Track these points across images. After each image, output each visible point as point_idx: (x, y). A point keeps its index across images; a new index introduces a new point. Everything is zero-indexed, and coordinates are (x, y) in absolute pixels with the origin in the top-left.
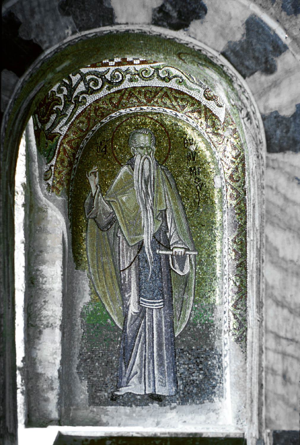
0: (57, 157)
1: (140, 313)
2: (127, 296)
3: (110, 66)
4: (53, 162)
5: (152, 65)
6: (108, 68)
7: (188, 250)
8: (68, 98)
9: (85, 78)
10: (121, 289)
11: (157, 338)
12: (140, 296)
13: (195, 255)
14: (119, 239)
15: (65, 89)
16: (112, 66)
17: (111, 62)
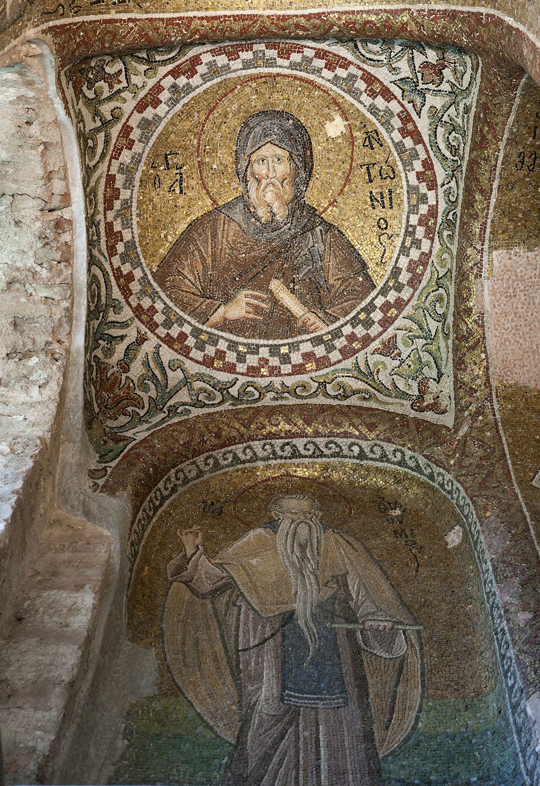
0: (122, 460)
1: (284, 715)
2: (250, 688)
3: (238, 373)
4: (113, 464)
5: (313, 374)
6: (234, 376)
7: (401, 623)
8: (156, 406)
9: (190, 383)
10: (236, 678)
11: (329, 760)
12: (284, 687)
13: (419, 632)
14: (240, 610)
15: (153, 387)
16: (242, 374)
17: (241, 365)
